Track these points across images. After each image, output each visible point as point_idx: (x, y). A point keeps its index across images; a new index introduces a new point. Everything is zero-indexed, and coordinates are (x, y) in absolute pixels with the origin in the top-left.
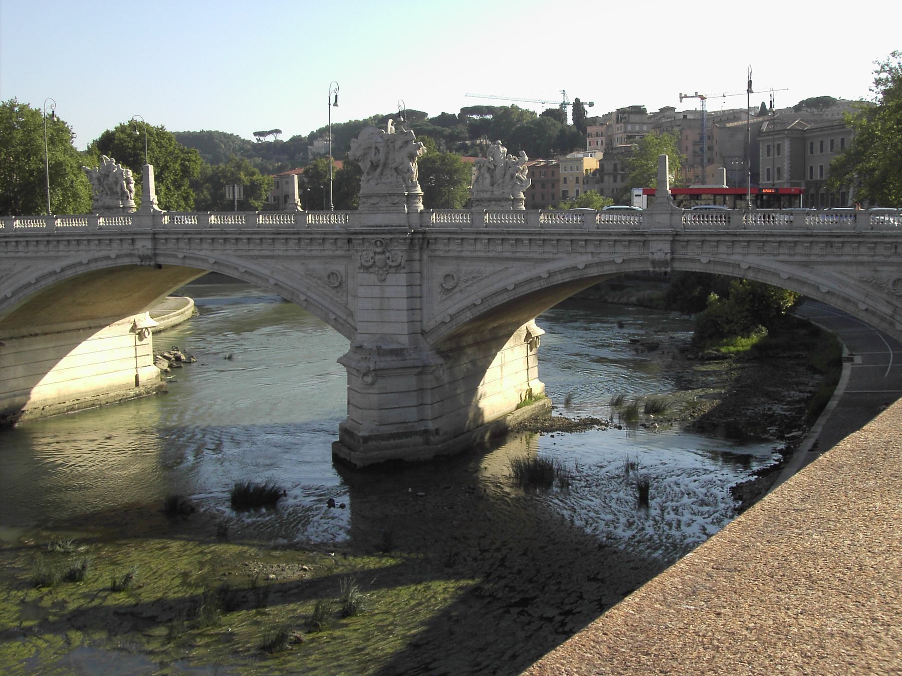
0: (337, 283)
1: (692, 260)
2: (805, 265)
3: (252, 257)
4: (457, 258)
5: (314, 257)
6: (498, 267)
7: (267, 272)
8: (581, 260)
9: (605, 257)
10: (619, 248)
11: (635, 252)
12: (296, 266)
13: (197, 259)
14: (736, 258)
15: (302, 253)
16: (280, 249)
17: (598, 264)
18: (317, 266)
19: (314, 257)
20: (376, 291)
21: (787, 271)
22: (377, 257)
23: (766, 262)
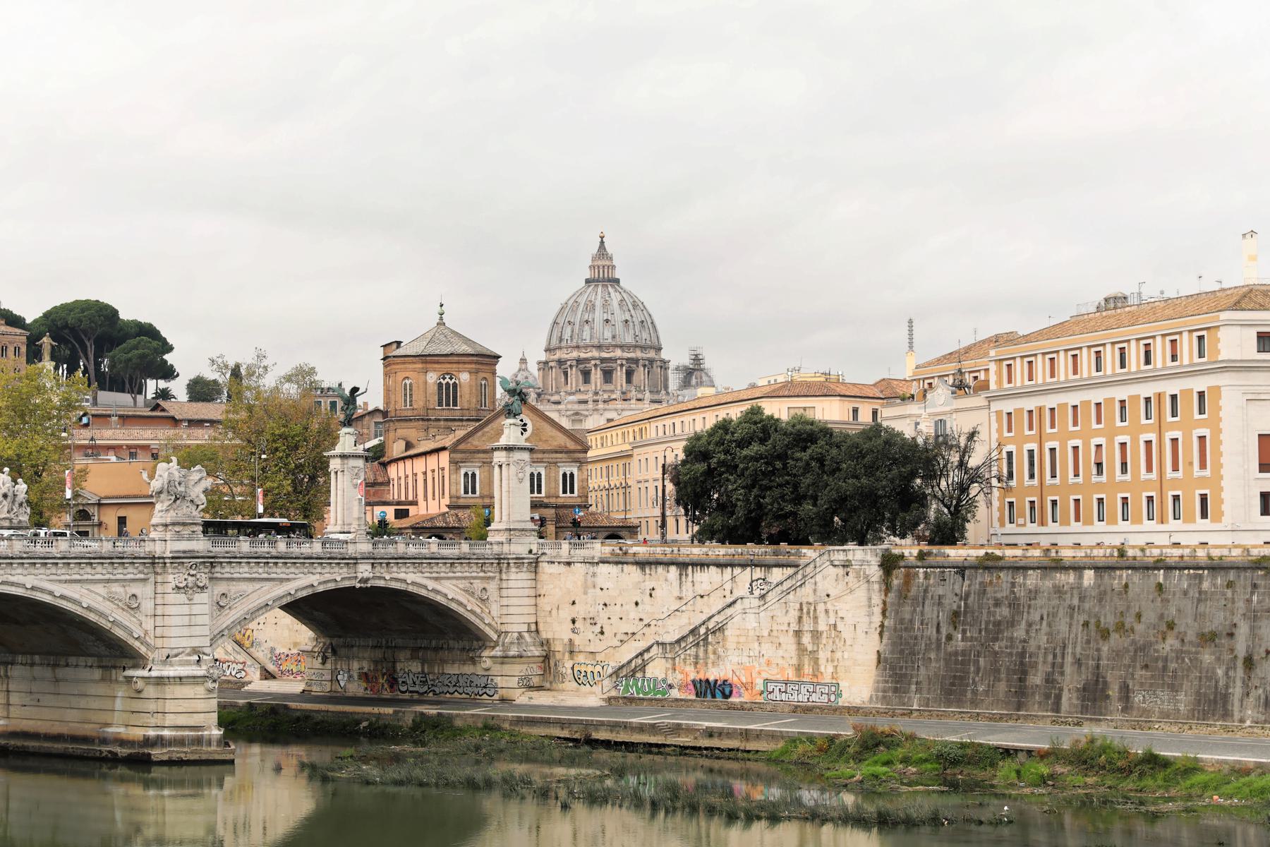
0: (132, 606)
1: (380, 578)
2: (436, 579)
3: (60, 581)
4: (228, 579)
5: (117, 581)
6: (257, 585)
7: (76, 596)
8: (314, 579)
9: (328, 577)
10: (336, 570)
11: (344, 572)
12: (99, 588)
13: (12, 584)
14: (402, 576)
15: (107, 576)
16: (87, 573)
17: (325, 582)
18: (116, 588)
19: (117, 581)
20: (185, 610)
21: (431, 585)
22: (190, 579)
23: (418, 578)
